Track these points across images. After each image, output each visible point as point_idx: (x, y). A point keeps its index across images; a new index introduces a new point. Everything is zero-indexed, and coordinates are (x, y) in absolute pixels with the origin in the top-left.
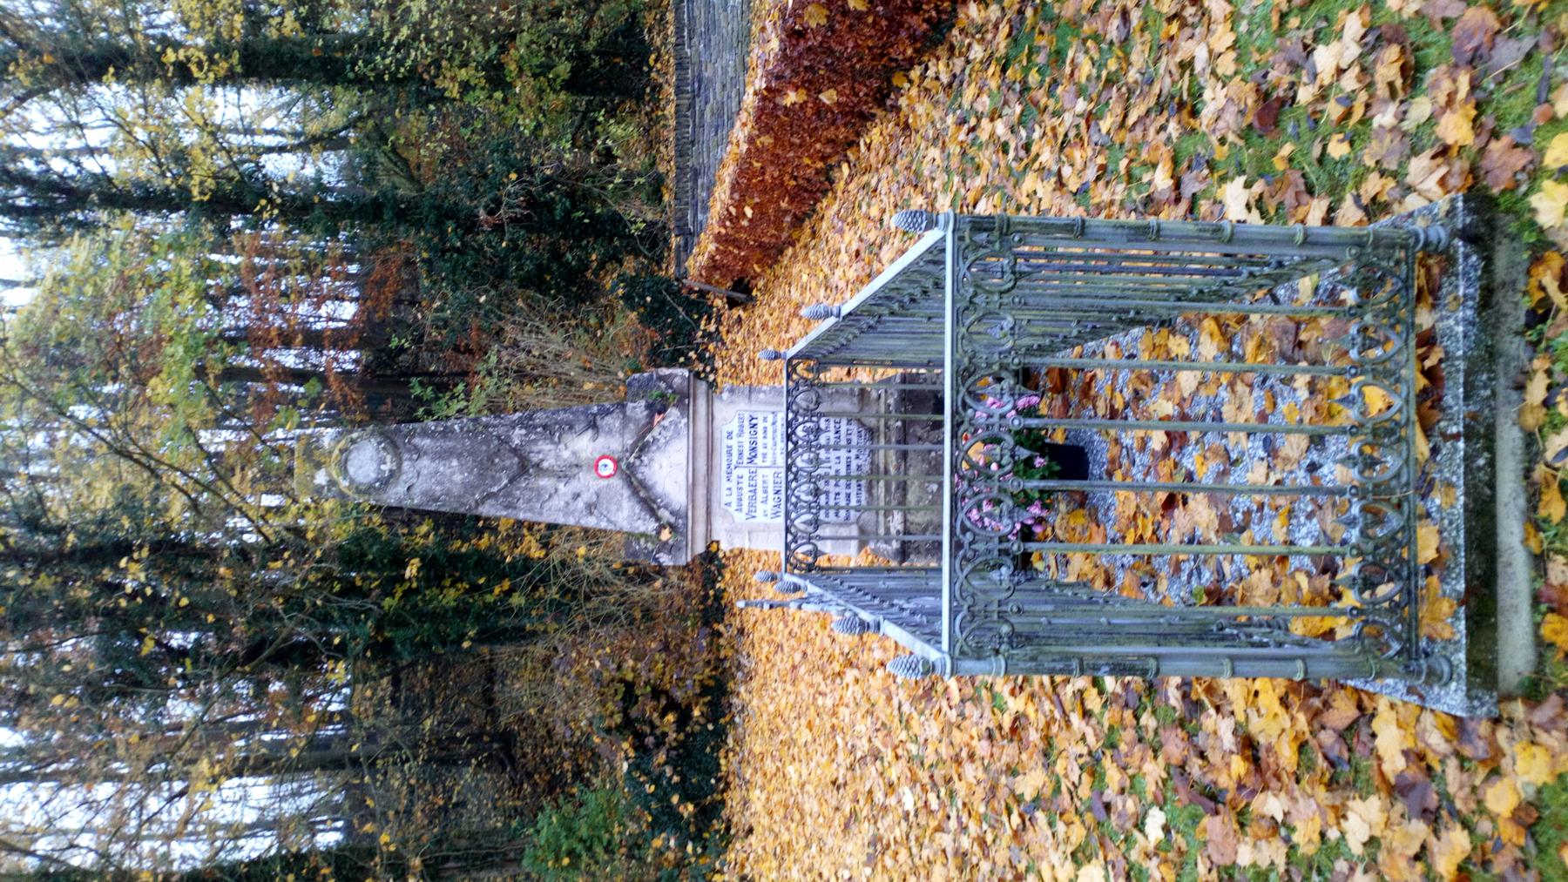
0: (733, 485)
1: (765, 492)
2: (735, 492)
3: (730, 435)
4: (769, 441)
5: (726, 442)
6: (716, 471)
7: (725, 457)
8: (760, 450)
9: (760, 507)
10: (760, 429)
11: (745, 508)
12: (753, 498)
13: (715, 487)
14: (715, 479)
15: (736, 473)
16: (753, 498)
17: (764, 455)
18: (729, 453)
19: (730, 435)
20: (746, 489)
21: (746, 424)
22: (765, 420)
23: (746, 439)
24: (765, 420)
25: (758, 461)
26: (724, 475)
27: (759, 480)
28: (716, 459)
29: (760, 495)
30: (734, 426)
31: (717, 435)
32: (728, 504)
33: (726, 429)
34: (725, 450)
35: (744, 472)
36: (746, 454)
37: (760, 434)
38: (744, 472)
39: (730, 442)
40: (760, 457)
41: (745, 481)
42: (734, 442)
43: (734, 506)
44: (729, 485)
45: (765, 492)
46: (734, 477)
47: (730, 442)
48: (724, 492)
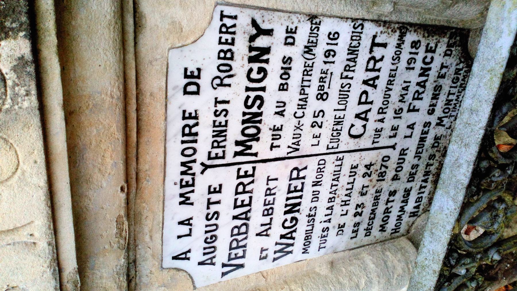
0: (197, 212)
1: (268, 212)
2: (200, 226)
3: (192, 77)
4: (292, 97)
5: (180, 102)
6: (150, 185)
7: (175, 147)
8: (269, 119)
9: (254, 244)
10: (274, 67)
11: (222, 255)
12: (239, 233)
13: (148, 224)
14: (148, 208)
15: (203, 182)
16: (239, 233)
17: (277, 130)
18: (189, 134)
19: (192, 77)
20: (226, 210)
21: (241, 48)
22: (290, 38)
23: (236, 94)
24: (290, 38)
25: (261, 148)
26: (173, 191)
27: (259, 189)
28: (151, 154)
29: (257, 219)
30: (205, 56)
31: (153, 82)
32: (183, 256)
33: (179, 62)
34: (177, 124)
35: (227, 178)
36: (234, 131)
37: (272, 82)
38: (227, 178)
39: (191, 104)
40: (266, 136)
41: (227, 197)
42: (203, 104)
43: (197, 256)
44: (185, 212)
45: (268, 212)
46: (199, 195)
47: (191, 104)
48: (173, 229)
